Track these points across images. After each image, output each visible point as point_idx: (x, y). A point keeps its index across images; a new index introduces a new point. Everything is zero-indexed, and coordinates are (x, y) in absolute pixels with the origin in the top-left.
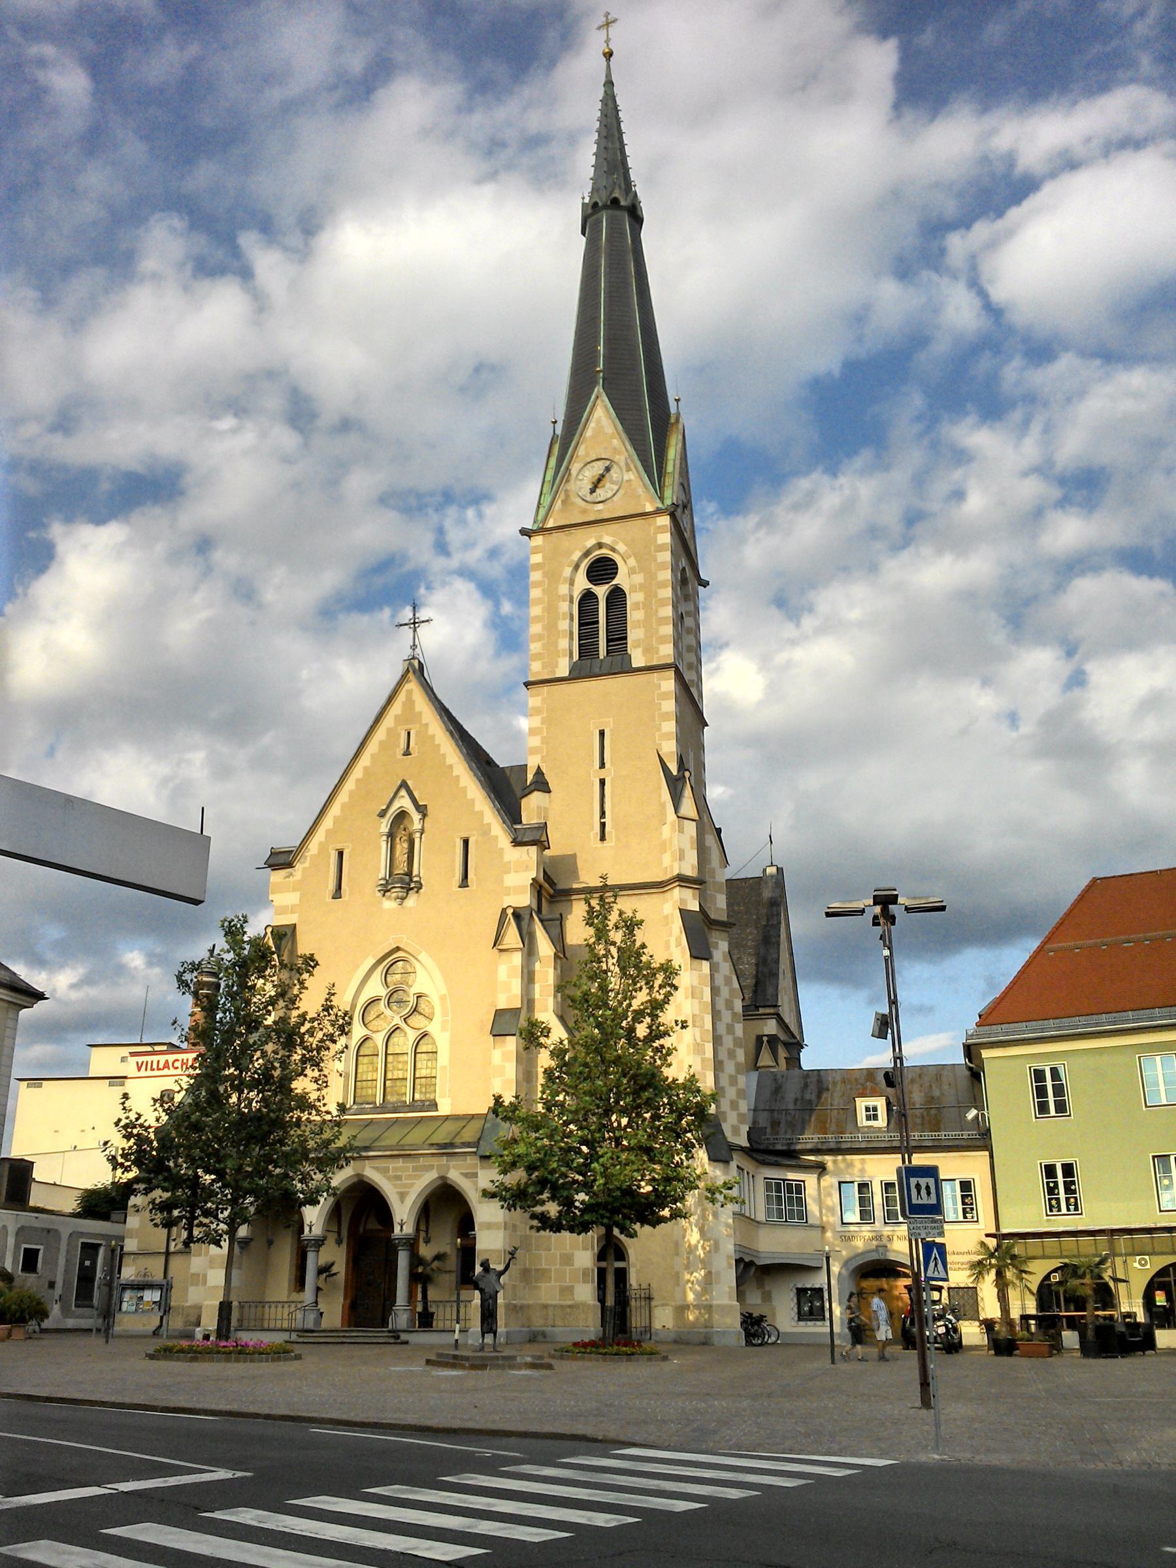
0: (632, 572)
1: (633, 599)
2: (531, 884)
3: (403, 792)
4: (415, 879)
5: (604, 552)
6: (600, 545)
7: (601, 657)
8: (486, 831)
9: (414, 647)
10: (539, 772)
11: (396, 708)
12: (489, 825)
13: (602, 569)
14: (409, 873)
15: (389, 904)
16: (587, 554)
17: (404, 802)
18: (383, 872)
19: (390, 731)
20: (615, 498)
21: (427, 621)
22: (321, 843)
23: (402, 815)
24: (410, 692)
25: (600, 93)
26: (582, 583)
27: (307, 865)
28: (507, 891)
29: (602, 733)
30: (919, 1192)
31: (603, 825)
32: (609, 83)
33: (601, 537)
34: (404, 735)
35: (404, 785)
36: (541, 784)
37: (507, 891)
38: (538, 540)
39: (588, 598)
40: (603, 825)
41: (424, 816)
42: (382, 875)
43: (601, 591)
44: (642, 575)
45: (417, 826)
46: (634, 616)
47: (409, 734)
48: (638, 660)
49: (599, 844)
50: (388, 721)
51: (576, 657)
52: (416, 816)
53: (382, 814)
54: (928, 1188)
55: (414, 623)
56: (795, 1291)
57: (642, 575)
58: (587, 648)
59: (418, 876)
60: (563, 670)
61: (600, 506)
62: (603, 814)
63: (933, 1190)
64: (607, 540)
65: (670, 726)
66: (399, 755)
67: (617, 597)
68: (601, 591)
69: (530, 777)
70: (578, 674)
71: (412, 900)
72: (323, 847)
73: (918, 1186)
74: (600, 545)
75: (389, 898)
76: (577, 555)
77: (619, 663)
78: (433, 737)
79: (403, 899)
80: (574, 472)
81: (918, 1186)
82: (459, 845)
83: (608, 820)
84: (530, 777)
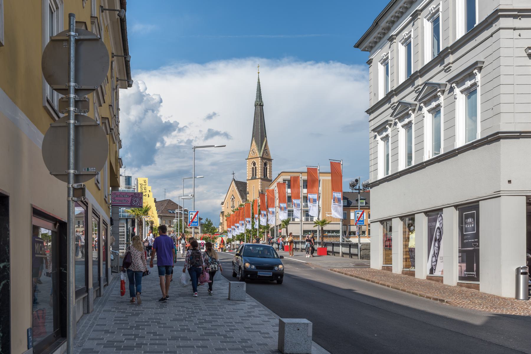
1: (257, 169)
6: (254, 161)
8: (240, 200)
10: (248, 192)
11: (232, 185)
13: (254, 164)
16: (252, 162)
17: (233, 197)
26: (252, 166)
32: (259, 78)
35: (233, 195)
36: (248, 193)
38: (248, 160)
39: (253, 168)
43: (254, 167)
48: (257, 178)
50: (231, 187)
51: (252, 176)
58: (253, 175)
64: (254, 161)
65: (260, 186)
72: (226, 202)
74: (254, 161)
76: (251, 162)
77: (256, 179)
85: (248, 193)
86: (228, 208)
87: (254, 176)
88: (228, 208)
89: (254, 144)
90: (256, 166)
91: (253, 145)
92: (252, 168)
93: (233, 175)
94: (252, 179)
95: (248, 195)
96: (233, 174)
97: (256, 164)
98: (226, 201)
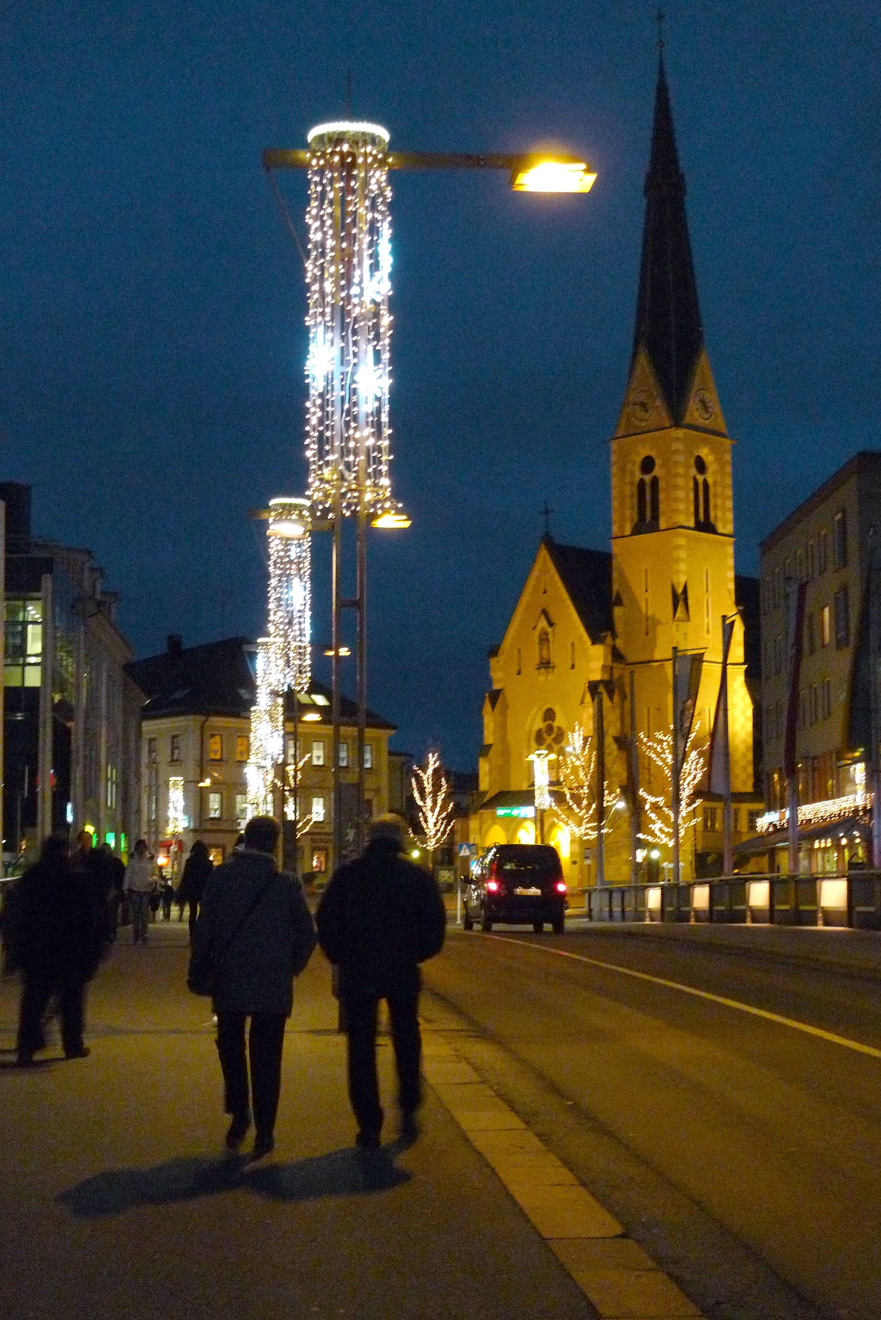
1: (662, 484)
3: (543, 618)
10: (618, 594)
15: (542, 679)
17: (543, 623)
27: (505, 656)
35: (545, 613)
39: (641, 484)
41: (554, 631)
43: (648, 478)
51: (636, 519)
52: (550, 630)
53: (534, 628)
61: (643, 424)
67: (655, 481)
68: (648, 478)
69: (614, 597)
71: (550, 677)
79: (547, 676)
89: (647, 371)
90: (657, 471)
94: (637, 530)
95: (617, 611)
97: (658, 462)
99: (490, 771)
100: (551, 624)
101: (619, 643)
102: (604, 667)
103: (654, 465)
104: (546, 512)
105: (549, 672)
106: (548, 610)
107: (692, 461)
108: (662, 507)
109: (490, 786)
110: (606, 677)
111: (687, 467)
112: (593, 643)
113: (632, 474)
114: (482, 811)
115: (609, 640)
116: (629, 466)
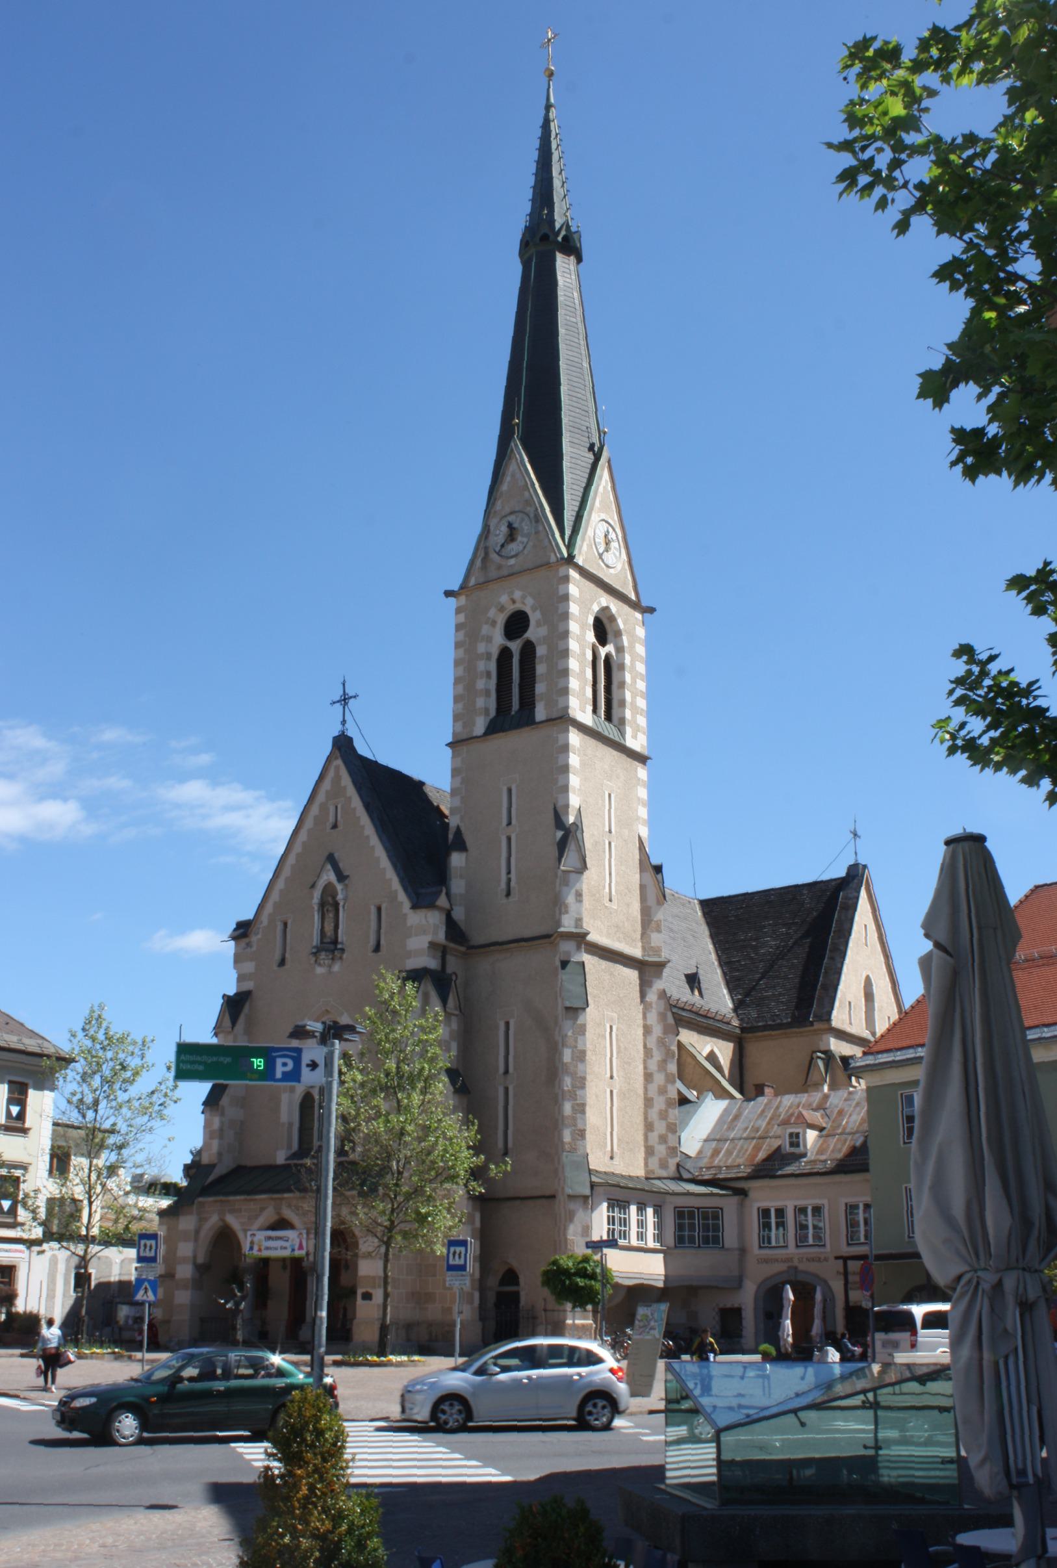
0: (538, 624)
1: (541, 651)
2: (429, 947)
3: (329, 867)
4: (339, 946)
5: (518, 606)
7: (513, 713)
8: (393, 897)
9: (344, 722)
10: (458, 831)
12: (396, 891)
13: (517, 624)
14: (335, 942)
15: (320, 970)
17: (330, 876)
18: (316, 941)
19: (323, 808)
20: (526, 552)
21: (355, 697)
22: (270, 915)
23: (329, 890)
24: (337, 768)
25: (540, 122)
27: (259, 936)
28: (409, 954)
29: (510, 791)
30: (145, 1250)
31: (509, 880)
33: (512, 593)
34: (332, 810)
35: (331, 859)
36: (460, 844)
37: (409, 954)
39: (505, 654)
40: (509, 880)
42: (314, 944)
43: (515, 646)
44: (546, 627)
45: (340, 897)
46: (541, 669)
47: (336, 807)
49: (504, 901)
51: (493, 713)
52: (339, 887)
53: (313, 886)
54: (151, 1247)
55: (345, 700)
56: (717, 1310)
57: (546, 627)
59: (342, 943)
60: (480, 727)
61: (512, 561)
62: (509, 872)
63: (154, 1248)
66: (328, 830)
67: (529, 650)
70: (494, 728)
71: (336, 967)
73: (145, 1246)
75: (320, 965)
78: (354, 809)
79: (330, 966)
80: (492, 528)
81: (145, 1246)
82: (373, 910)
83: (513, 876)
84: (451, 836)
85: (460, 844)
86: (282, 963)
87: (515, 705)
88: (282, 963)
90: (532, 633)
91: (504, 487)
92: (495, 652)
93: (338, 708)
95: (457, 860)
96: (345, 700)
97: (534, 617)
98: (269, 908)
99: (221, 1130)
100: (341, 877)
101: (459, 914)
102: (433, 945)
103: (528, 621)
104: (345, 700)
105: (333, 959)
106: (336, 855)
107: (591, 620)
108: (540, 688)
109: (220, 1154)
110: (432, 964)
111: (583, 627)
112: (415, 907)
113: (489, 639)
114: (201, 1199)
115: (442, 901)
116: (485, 629)
